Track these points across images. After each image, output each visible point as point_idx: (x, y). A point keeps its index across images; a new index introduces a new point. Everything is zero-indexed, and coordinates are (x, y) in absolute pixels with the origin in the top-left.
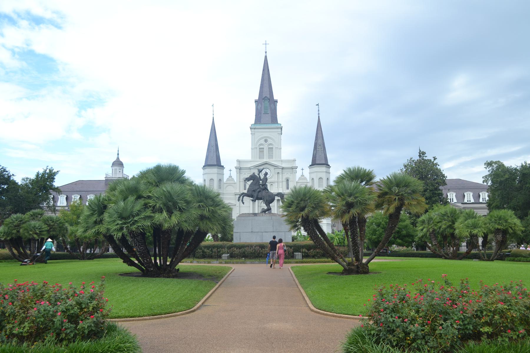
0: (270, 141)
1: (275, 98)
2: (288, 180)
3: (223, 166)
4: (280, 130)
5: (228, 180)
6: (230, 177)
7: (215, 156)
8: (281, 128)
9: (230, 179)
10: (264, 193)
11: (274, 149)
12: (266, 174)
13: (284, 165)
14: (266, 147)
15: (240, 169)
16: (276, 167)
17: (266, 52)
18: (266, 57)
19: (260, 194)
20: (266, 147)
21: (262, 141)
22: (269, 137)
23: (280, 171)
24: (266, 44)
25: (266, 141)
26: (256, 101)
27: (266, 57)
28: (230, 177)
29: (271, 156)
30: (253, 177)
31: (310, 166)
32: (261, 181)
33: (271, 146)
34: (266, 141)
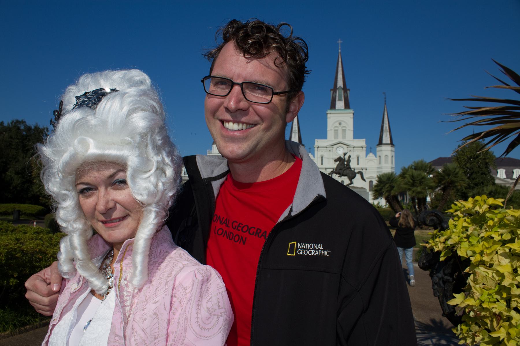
0: (343, 124)
2: (358, 157)
10: (348, 171)
12: (350, 157)
14: (340, 129)
16: (348, 146)
19: (345, 171)
20: (340, 129)
21: (337, 124)
23: (351, 149)
25: (340, 124)
29: (344, 137)
30: (339, 159)
31: (378, 145)
32: (346, 163)
33: (344, 128)
34: (340, 124)
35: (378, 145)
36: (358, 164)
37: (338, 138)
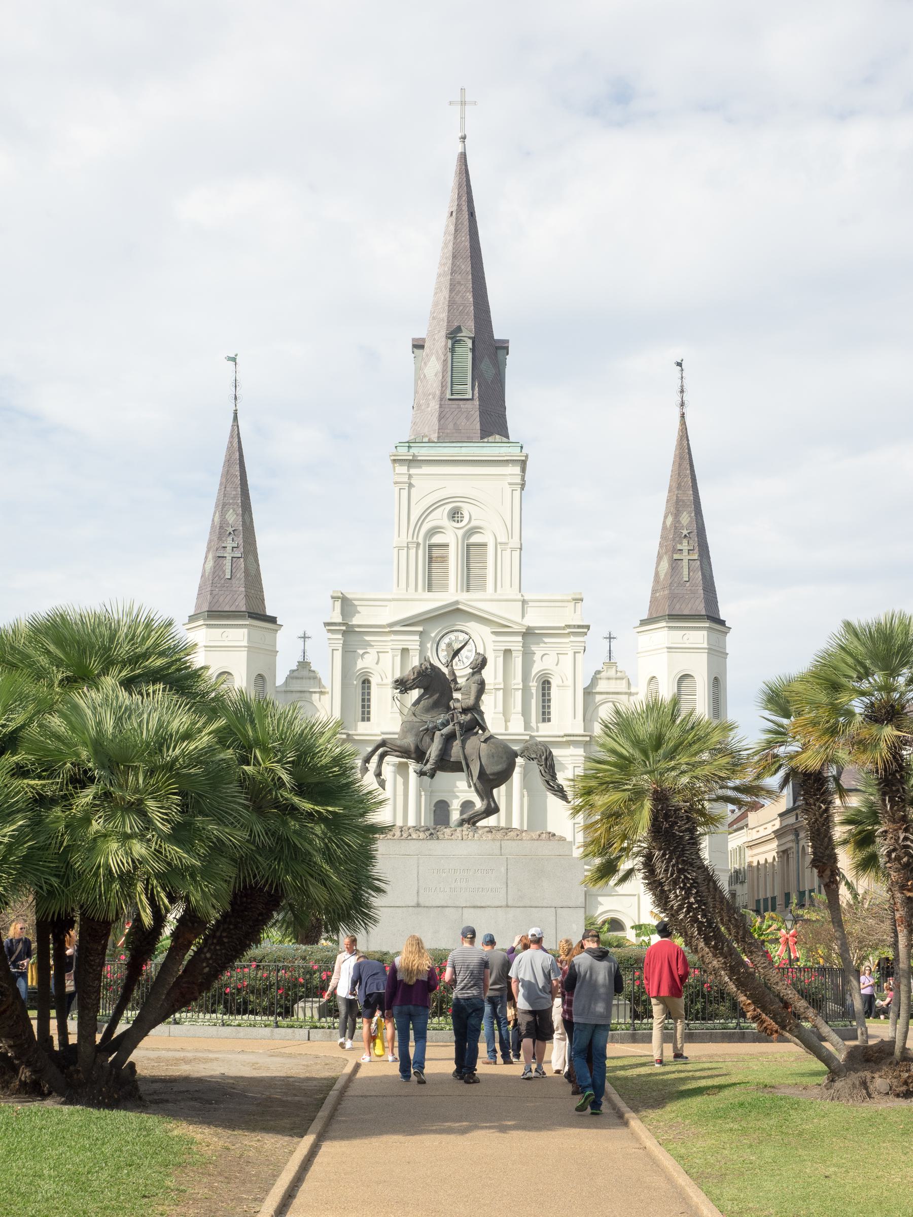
1: (497, 336)
3: (273, 620)
4: (517, 470)
5: (293, 676)
6: (304, 664)
7: (240, 574)
8: (523, 464)
9: (305, 673)
11: (490, 550)
12: (480, 664)
13: (534, 619)
15: (344, 633)
17: (464, 138)
18: (463, 157)
21: (440, 517)
22: (466, 499)
23: (516, 643)
24: (463, 103)
26: (418, 346)
27: (463, 157)
28: (304, 664)
31: (644, 622)
35: (644, 622)
36: (545, 716)
37: (444, 587)
